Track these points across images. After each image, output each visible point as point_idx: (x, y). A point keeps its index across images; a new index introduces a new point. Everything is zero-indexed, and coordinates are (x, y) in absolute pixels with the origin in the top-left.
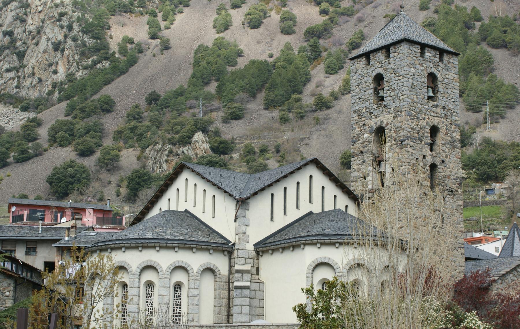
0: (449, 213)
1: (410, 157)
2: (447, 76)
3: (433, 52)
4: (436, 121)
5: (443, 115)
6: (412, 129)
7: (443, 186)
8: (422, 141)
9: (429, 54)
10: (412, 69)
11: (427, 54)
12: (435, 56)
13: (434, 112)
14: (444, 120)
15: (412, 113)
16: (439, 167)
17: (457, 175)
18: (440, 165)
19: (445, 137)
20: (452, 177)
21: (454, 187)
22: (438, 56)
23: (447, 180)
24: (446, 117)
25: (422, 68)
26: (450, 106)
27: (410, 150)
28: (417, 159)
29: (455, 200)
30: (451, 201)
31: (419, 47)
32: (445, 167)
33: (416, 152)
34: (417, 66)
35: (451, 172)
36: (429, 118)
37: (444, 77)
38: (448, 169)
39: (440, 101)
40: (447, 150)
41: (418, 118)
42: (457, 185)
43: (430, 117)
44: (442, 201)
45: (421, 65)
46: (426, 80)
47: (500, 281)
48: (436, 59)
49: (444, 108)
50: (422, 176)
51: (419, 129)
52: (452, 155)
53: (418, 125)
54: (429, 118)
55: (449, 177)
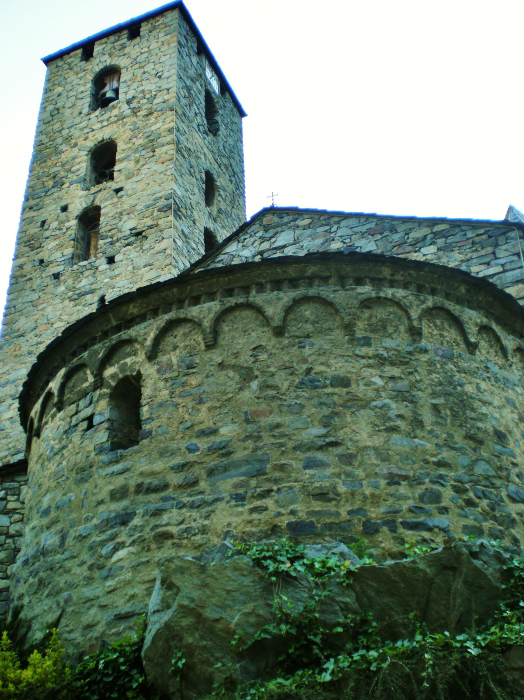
3: (112, 38)
29: (146, 246)
32: (121, 197)
42: (156, 213)
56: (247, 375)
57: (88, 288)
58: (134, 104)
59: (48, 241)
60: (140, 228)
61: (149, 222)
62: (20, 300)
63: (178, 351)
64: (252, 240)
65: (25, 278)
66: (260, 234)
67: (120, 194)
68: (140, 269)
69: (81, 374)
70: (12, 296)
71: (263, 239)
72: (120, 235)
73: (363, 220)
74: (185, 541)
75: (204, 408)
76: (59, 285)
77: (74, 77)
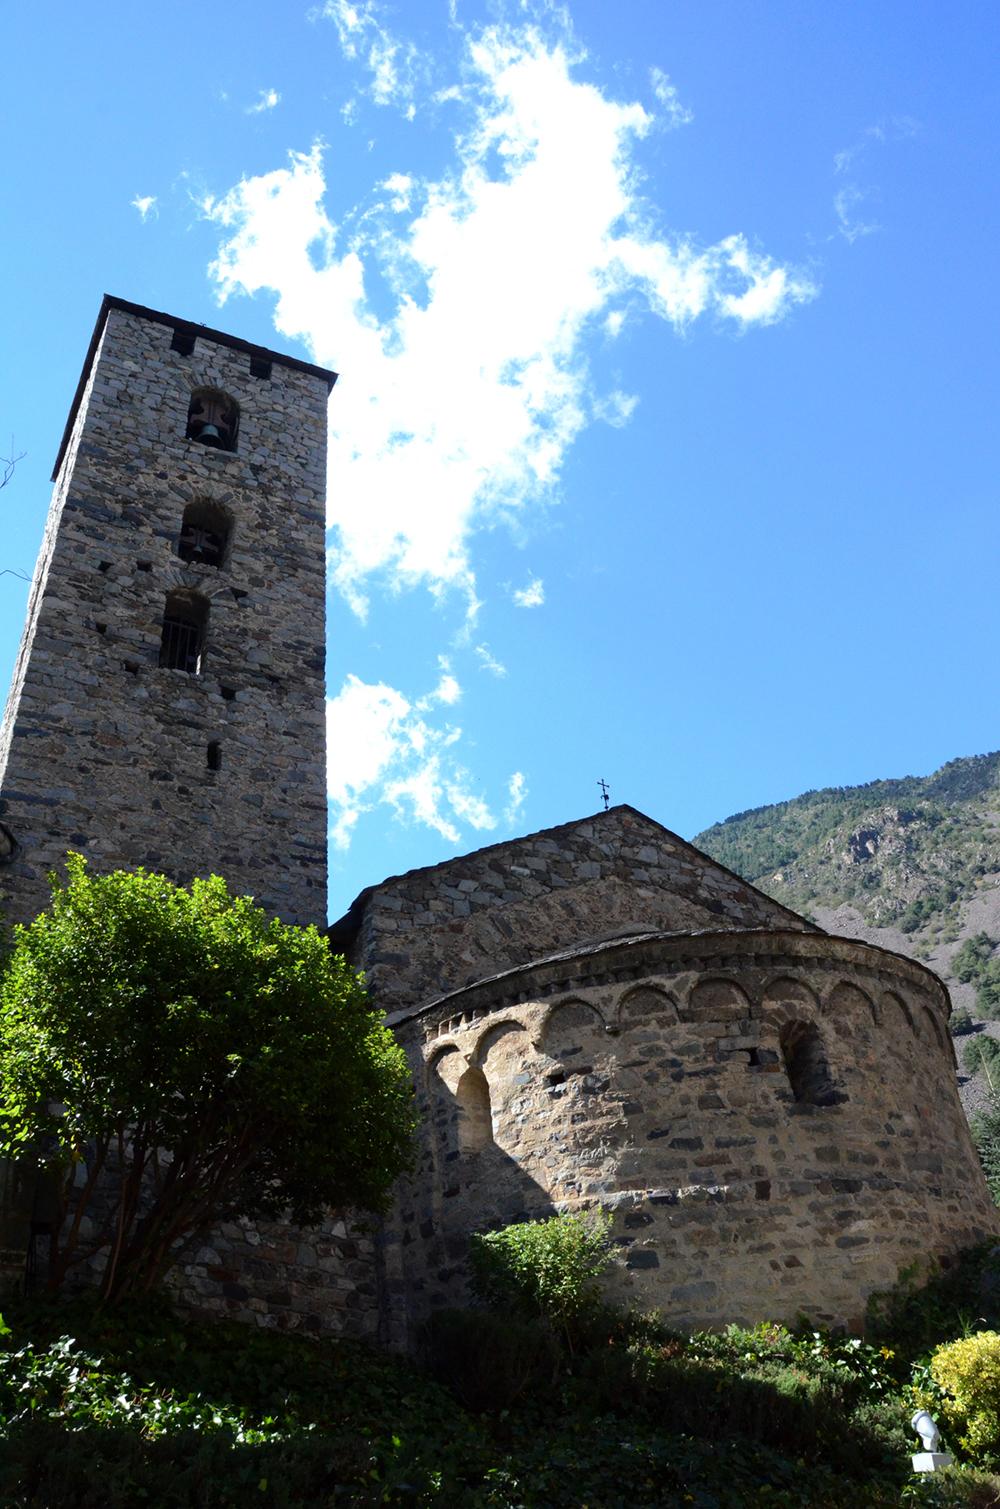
0: (247, 739)
1: (70, 554)
2: (277, 407)
3: (225, 351)
4: (218, 491)
5: (256, 483)
6: (96, 486)
7: (228, 657)
8: (140, 523)
9: (212, 353)
10: (130, 365)
11: (200, 347)
12: (231, 360)
13: (210, 470)
14: (254, 495)
15: (106, 453)
16: (213, 601)
17: (302, 638)
18: (219, 595)
19: (250, 534)
20: (279, 640)
21: (283, 668)
22: (249, 364)
23: (253, 643)
24: (266, 491)
25: (171, 370)
26: (283, 468)
27: (80, 536)
28: (104, 567)
30: (266, 705)
31: (172, 331)
32: (245, 606)
33: (101, 543)
34: (149, 363)
35: (273, 624)
36: (183, 478)
37: (264, 407)
38: (258, 613)
39: (240, 451)
40: (259, 566)
41: (130, 468)
42: (300, 663)
43: (191, 477)
44: (216, 697)
45: (173, 364)
46: (188, 398)
47: (398, 904)
48: (231, 364)
49: (256, 469)
50: (122, 612)
51: (137, 496)
52: (282, 583)
53: (128, 485)
54: (183, 478)
55: (262, 636)
56: (909, 1069)
57: (188, 716)
58: (264, 478)
59: (115, 601)
60: (278, 671)
61: (289, 668)
62: (62, 668)
63: (851, 1017)
64: (612, 837)
65: (71, 639)
66: (620, 833)
67: (239, 600)
68: (277, 733)
69: (722, 989)
70: (44, 656)
71: (624, 842)
72: (243, 664)
73: (727, 877)
74: (916, 1226)
75: (887, 1088)
76: (136, 684)
77: (159, 365)
